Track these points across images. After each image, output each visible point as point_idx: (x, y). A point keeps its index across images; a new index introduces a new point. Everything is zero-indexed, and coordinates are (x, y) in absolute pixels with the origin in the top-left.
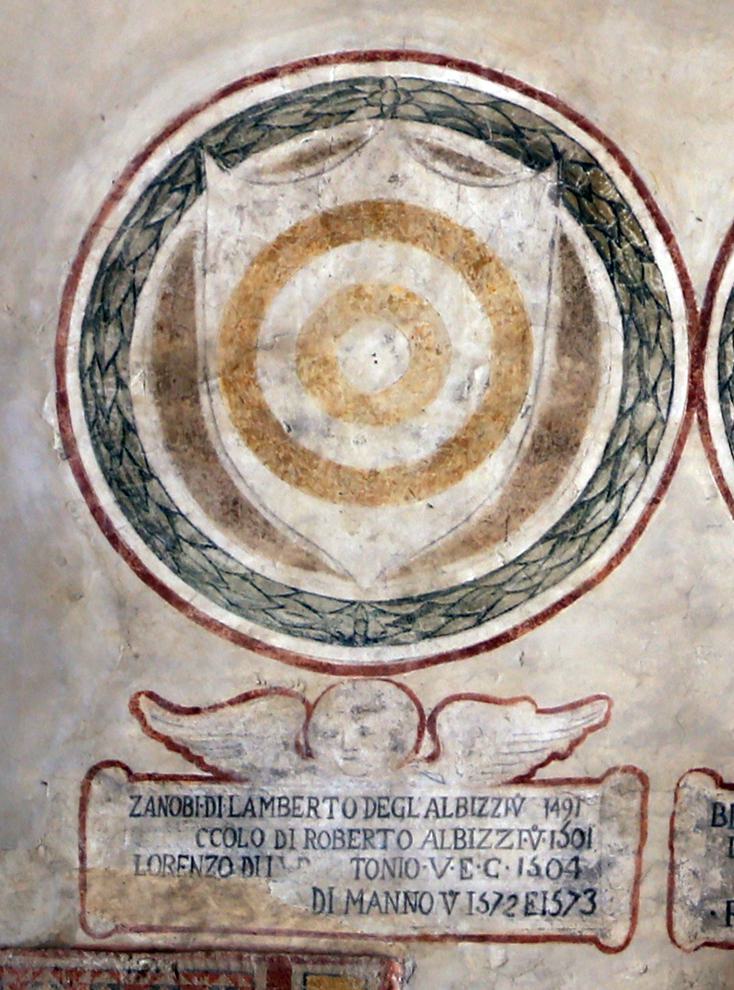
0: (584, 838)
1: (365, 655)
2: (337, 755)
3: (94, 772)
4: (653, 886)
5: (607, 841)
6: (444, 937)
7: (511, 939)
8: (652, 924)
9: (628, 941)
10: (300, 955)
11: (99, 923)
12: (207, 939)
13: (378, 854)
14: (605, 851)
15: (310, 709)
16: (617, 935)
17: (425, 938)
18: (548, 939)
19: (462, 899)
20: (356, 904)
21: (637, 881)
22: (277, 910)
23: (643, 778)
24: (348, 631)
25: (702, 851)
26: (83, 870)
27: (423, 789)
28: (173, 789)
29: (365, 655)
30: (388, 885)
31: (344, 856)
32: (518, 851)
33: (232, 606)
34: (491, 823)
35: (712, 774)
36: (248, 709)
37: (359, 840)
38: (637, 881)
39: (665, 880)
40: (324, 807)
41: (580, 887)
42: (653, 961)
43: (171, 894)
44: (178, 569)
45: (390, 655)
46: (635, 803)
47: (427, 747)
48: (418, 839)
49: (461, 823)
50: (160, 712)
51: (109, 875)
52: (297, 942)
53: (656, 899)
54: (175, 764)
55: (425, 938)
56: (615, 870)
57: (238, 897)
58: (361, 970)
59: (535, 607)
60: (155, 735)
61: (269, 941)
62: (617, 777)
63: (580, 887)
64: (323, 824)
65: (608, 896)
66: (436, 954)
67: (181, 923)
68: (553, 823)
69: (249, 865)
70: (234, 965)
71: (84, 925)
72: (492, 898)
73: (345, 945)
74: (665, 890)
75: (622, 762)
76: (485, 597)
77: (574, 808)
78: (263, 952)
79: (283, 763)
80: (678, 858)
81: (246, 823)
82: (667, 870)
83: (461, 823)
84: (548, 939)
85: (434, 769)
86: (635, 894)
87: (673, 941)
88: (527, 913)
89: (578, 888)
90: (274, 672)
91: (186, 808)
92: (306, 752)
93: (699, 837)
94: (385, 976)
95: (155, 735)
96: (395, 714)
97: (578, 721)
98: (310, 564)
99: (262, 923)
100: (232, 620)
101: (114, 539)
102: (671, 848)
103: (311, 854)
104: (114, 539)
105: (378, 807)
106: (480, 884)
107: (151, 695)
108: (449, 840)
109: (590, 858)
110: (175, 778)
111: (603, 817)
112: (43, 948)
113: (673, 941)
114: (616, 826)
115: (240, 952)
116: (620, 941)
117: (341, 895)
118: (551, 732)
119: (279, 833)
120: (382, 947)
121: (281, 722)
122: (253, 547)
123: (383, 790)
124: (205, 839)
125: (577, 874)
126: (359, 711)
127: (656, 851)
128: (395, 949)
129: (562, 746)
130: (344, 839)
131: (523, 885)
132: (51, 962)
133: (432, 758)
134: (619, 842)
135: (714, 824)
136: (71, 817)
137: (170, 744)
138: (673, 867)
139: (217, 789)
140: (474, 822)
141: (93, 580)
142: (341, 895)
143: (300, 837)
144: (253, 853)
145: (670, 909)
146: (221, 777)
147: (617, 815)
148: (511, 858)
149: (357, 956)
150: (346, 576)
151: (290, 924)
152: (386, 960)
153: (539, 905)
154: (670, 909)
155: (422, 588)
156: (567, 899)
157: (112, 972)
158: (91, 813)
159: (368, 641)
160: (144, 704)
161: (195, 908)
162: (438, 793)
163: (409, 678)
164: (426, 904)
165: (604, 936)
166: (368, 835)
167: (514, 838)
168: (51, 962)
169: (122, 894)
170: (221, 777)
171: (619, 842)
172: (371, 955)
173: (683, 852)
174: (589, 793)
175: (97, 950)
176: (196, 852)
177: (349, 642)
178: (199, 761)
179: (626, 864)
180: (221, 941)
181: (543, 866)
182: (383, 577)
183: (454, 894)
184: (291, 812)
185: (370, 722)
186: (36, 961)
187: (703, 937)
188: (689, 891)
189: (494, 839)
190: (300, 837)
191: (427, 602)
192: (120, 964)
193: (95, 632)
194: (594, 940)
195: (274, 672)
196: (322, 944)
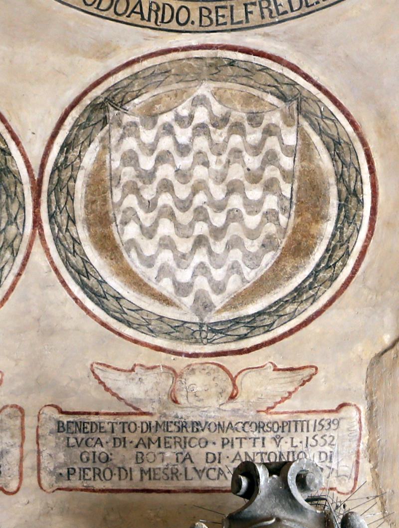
4: (30, 462)
8: (30, 480)
9: (18, 489)
16: (13, 486)
21: (21, 460)
23: (21, 410)
25: (53, 444)
35: (56, 407)
38: (21, 460)
39: (36, 459)
42: (31, 498)
46: (18, 422)
53: (32, 468)
56: (10, 455)
62: (8, 410)
65: (7, 467)
74: (36, 464)
75: (10, 403)
80: (41, 449)
82: (36, 454)
86: (21, 466)
87: (42, 488)
93: (51, 438)
102: (38, 443)
113: (42, 488)
114: (9, 434)
116: (15, 489)
127: (30, 445)
134: (11, 441)
135: (59, 431)
138: (39, 453)
145: (39, 473)
147: (9, 428)
154: (39, 473)
165: (6, 487)
171: (11, 441)
173: (44, 445)
179: (15, 452)
187: (56, 486)
188: (48, 464)
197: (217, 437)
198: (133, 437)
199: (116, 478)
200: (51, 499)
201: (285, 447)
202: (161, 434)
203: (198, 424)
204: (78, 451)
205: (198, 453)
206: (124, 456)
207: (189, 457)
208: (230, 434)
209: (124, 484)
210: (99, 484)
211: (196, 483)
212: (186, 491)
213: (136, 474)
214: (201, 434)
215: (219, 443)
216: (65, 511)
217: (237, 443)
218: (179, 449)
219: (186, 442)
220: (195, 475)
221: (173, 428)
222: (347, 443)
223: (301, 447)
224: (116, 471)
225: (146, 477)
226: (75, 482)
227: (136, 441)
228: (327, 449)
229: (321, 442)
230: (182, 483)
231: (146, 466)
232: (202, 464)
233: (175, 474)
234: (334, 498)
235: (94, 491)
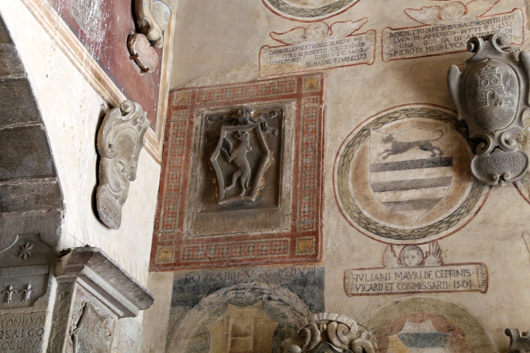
0: (363, 44)
1: (317, 18)
2: (311, 37)
3: (262, 48)
4: (378, 50)
5: (368, 44)
6: (334, 68)
7: (348, 66)
9: (373, 62)
10: (304, 75)
11: (263, 75)
12: (285, 75)
13: (320, 54)
14: (368, 46)
15: (305, 30)
16: (371, 61)
17: (330, 68)
18: (356, 64)
19: (338, 60)
20: (316, 64)
21: (375, 50)
22: (299, 68)
23: (375, 31)
24: (313, 14)
26: (259, 66)
27: (329, 40)
28: (278, 49)
29: (317, 18)
30: (322, 60)
31: (313, 55)
32: (350, 48)
33: (290, 14)
34: (343, 45)
35: (390, 28)
36: (293, 32)
37: (316, 52)
38: (375, 50)
40: (309, 47)
41: (363, 54)
43: (277, 68)
44: (279, 9)
45: (321, 17)
46: (374, 36)
47: (330, 32)
48: (328, 50)
49: (337, 46)
50: (275, 35)
51: (265, 66)
52: (303, 73)
53: (379, 53)
54: (279, 44)
55: (330, 68)
57: (291, 66)
58: (317, 76)
59: (351, 4)
60: (274, 39)
61: (298, 74)
62: (370, 32)
63: (363, 54)
64: (309, 50)
66: (333, 70)
67: (279, 73)
68: (357, 42)
69: (293, 60)
70: (290, 79)
71: (259, 76)
72: (344, 59)
73: (313, 72)
75: (370, 29)
76: (341, 4)
77: (360, 39)
78: (296, 76)
79: (300, 40)
80: (383, 45)
81: (293, 52)
83: (337, 46)
84: (356, 64)
85: (331, 36)
88: (352, 60)
89: (362, 53)
90: (298, 24)
91: (280, 52)
92: (305, 37)
93: (388, 40)
94: (322, 77)
95: (274, 39)
96: (323, 27)
97: (360, 23)
98: (305, 4)
99: (296, 71)
100: (290, 16)
101: (266, 6)
103: (306, 56)
104: (266, 6)
105: (319, 45)
106: (341, 56)
107: (273, 32)
108: (335, 49)
109: (364, 48)
110: (278, 46)
111: (367, 40)
112: (251, 82)
115: (291, 77)
117: (312, 63)
118: (355, 26)
119: (300, 53)
120: (321, 71)
121: (300, 32)
122: (294, 3)
123: (321, 42)
124: (284, 57)
125: (362, 51)
126: (316, 28)
127: (378, 44)
128: (324, 71)
129: (358, 28)
130: (313, 52)
131: (350, 55)
132: (253, 84)
133: (331, 34)
134: (371, 44)
136: (257, 57)
137: (277, 40)
138: (382, 47)
139: (287, 47)
140: (340, 45)
141: (262, 14)
142: (312, 63)
143: (304, 53)
144: (294, 58)
146: (287, 45)
148: (348, 50)
149: (316, 74)
150: (313, 5)
151: (302, 70)
152: (322, 74)
153: (354, 58)
155: (328, 4)
156: (360, 56)
157: (265, 84)
158: (261, 55)
159: (317, 15)
160: (272, 34)
161: (282, 70)
162: (332, 41)
163: (325, 21)
164: (330, 62)
166: (318, 51)
167: (348, 47)
168: (253, 84)
169: (267, 69)
170: (287, 45)
171: (371, 44)
172: (319, 73)
174: (364, 35)
175: (262, 81)
176: (282, 59)
177: (313, 16)
178: (283, 43)
179: (372, 48)
180: (288, 75)
181: (354, 50)
182: (320, 4)
183: (336, 59)
184: (302, 49)
185: (318, 30)
186: (250, 84)
187: (390, 59)
189: (344, 47)
190: (304, 53)
191: (329, 7)
192: (267, 83)
193: (263, 23)
194: (366, 63)
195: (298, 24)
196: (308, 73)
197: (459, 30)
198: (422, 35)
199: (415, 52)
200: (388, 65)
201: (490, 30)
202: (435, 32)
203: (451, 26)
204: (399, 44)
205: (451, 38)
206: (419, 43)
207: (447, 40)
208: (465, 28)
209: (419, 54)
210: (408, 56)
211: (451, 50)
212: (447, 53)
213: (424, 50)
214: (452, 30)
215: (460, 32)
216: (393, 69)
217: (468, 31)
218: (442, 37)
219: (446, 34)
220: (450, 46)
221: (439, 29)
222: (518, 24)
223: (497, 29)
224: (415, 50)
225: (429, 50)
226: (398, 56)
227: (424, 37)
228: (509, 28)
229: (506, 25)
230: (445, 50)
231: (428, 46)
232: (453, 42)
233: (441, 47)
234: (514, 48)
235: (406, 59)
